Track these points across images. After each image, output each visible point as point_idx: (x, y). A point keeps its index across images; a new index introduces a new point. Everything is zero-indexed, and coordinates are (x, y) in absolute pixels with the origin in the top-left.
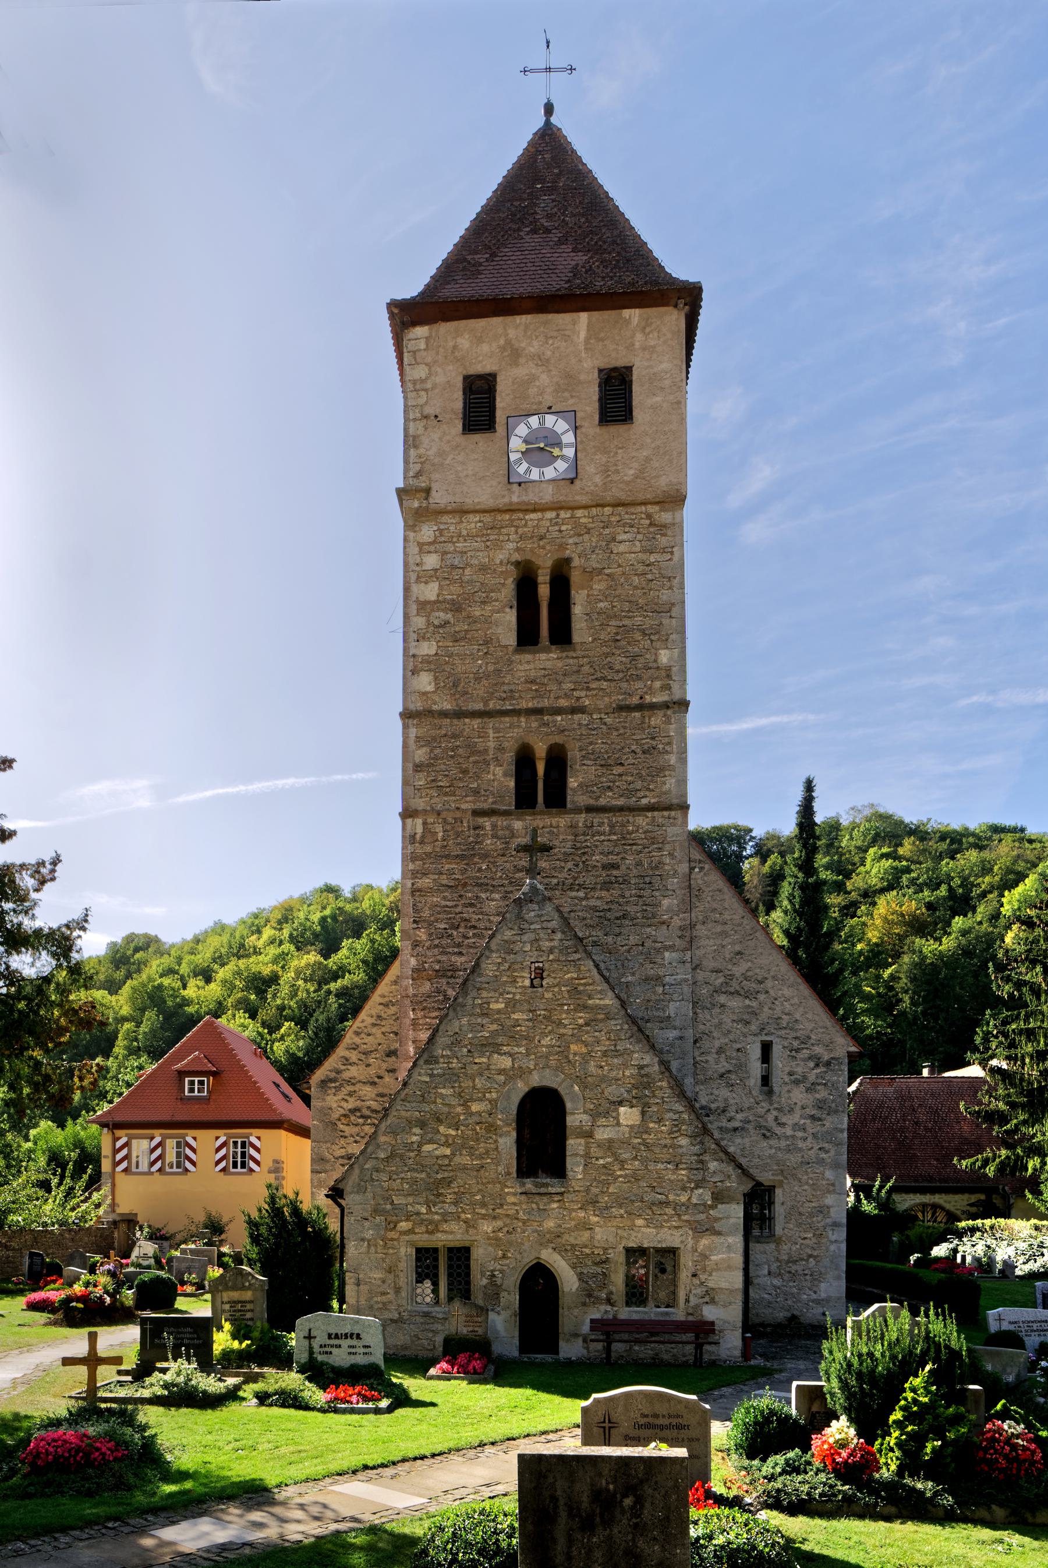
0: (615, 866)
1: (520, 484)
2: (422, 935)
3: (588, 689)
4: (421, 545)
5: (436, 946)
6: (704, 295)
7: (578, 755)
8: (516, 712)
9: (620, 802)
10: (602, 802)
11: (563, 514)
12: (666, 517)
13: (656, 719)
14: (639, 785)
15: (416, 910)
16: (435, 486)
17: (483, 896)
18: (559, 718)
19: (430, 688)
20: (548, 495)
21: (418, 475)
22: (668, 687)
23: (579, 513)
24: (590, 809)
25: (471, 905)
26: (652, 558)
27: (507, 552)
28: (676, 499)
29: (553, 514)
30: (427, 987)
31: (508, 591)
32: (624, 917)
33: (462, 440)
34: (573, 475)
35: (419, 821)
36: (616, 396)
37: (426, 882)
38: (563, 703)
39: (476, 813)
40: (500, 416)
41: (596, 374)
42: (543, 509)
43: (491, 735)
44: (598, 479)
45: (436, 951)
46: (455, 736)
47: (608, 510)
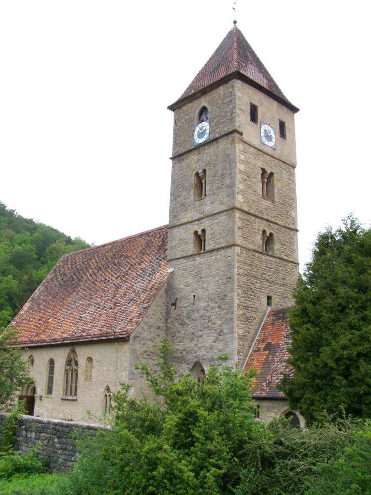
0: (285, 279)
1: (264, 144)
2: (240, 291)
3: (278, 217)
4: (240, 150)
5: (244, 297)
6: (298, 112)
7: (276, 239)
8: (262, 219)
9: (285, 257)
10: (282, 256)
11: (272, 159)
12: (291, 170)
13: (292, 233)
14: (289, 253)
15: (238, 282)
16: (244, 133)
17: (256, 281)
18: (272, 224)
19: (242, 201)
20: (269, 151)
21: (239, 127)
22: (294, 224)
23: (275, 160)
24: (280, 258)
25: (252, 283)
26: (290, 182)
27: (260, 164)
28: (294, 167)
29: (269, 157)
30: (241, 312)
31: (259, 177)
32: (286, 297)
33: (249, 121)
34: (275, 148)
35: (239, 248)
36: (282, 129)
37: (241, 271)
38: (273, 220)
39: (254, 251)
40: (259, 120)
41: (278, 121)
42: (268, 155)
43: (257, 224)
44: (280, 152)
45: (244, 299)
46: (248, 221)
47: (281, 163)
